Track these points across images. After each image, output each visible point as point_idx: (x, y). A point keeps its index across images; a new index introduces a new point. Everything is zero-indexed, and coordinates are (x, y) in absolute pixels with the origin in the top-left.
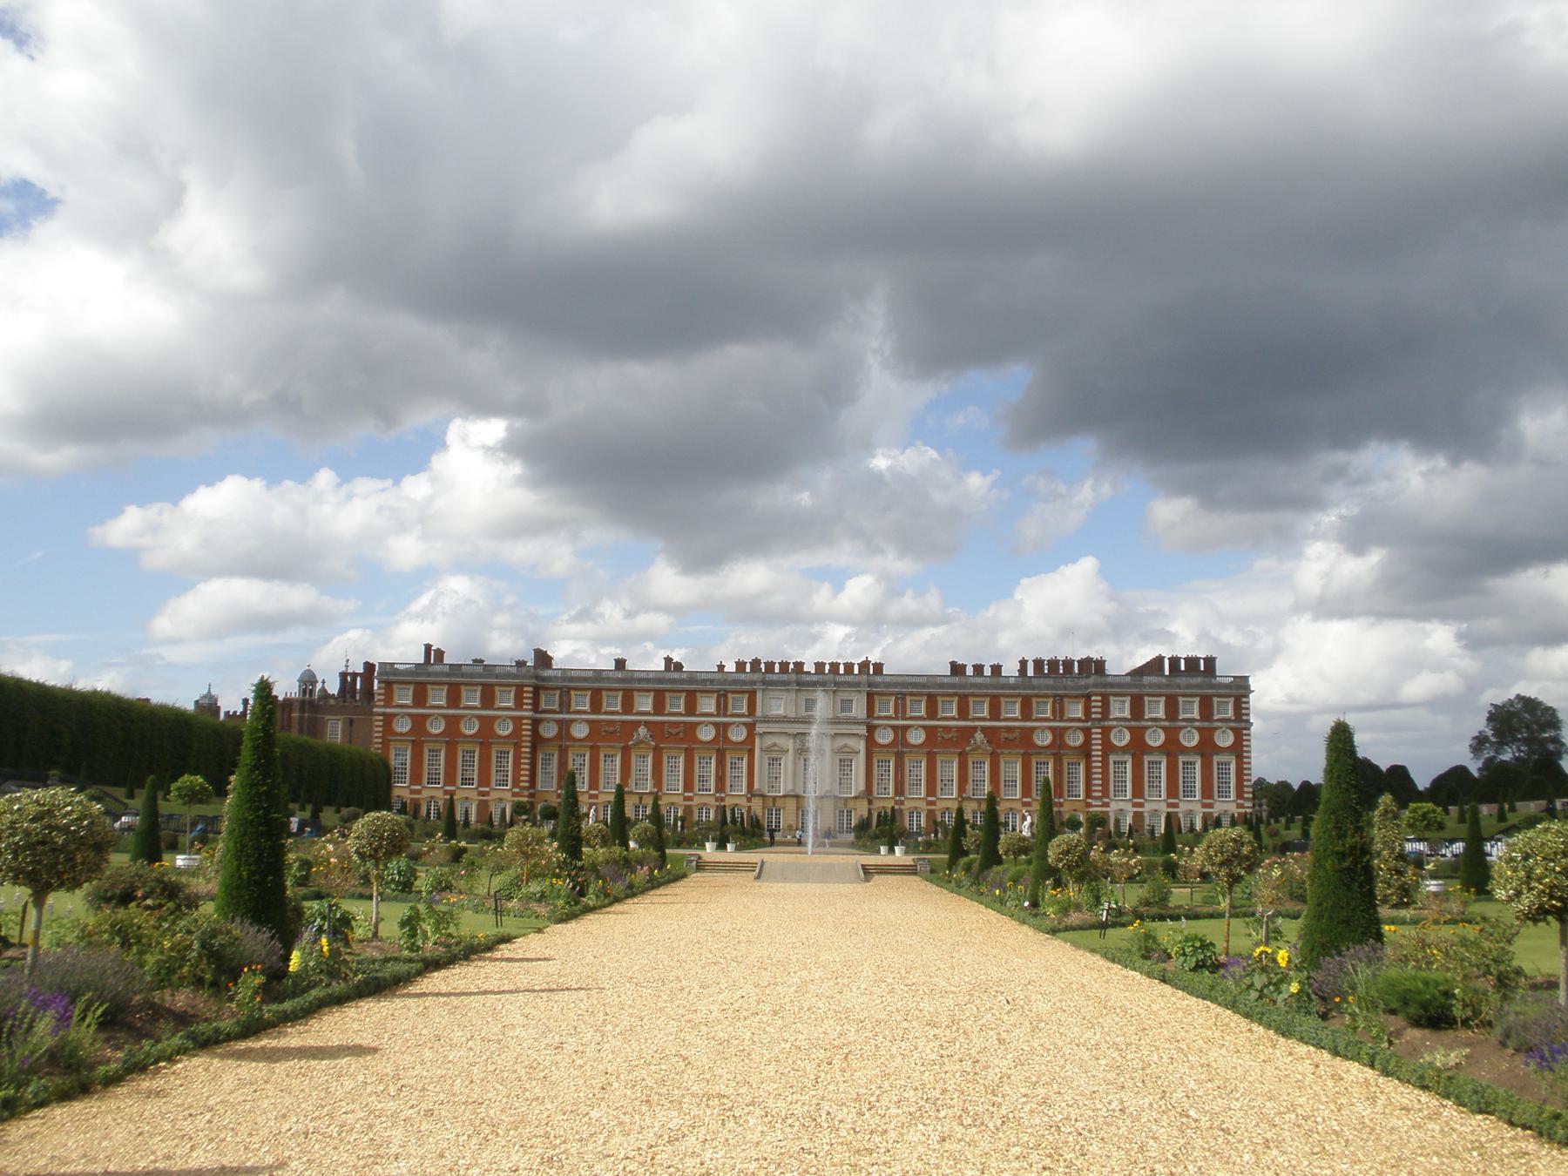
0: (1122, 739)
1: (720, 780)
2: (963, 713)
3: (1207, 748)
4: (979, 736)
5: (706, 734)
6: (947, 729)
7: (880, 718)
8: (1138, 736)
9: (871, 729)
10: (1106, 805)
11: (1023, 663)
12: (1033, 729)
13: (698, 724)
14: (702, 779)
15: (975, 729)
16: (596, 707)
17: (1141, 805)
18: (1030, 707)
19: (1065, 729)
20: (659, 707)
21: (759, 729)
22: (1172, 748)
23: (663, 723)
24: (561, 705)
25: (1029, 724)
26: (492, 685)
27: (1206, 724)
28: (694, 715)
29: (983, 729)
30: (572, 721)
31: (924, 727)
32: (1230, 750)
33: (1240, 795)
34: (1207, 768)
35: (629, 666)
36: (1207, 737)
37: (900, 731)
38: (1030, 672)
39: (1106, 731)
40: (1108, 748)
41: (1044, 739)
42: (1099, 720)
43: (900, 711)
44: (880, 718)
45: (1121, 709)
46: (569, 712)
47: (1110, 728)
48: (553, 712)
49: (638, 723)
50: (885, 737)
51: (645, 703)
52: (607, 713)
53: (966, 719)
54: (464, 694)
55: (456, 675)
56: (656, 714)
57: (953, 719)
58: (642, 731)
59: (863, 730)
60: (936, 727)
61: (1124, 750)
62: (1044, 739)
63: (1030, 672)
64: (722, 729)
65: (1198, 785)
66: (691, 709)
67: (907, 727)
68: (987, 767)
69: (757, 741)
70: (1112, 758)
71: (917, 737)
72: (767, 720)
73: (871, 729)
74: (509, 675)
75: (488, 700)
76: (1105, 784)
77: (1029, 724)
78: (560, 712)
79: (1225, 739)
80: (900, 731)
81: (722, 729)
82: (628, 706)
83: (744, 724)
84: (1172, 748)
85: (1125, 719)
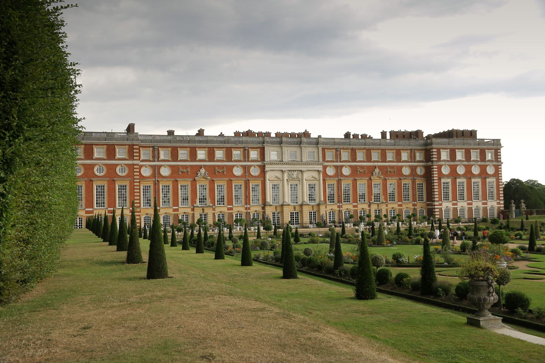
0: (445, 171)
1: (247, 197)
2: (369, 158)
3: (484, 175)
4: (377, 170)
5: (238, 172)
6: (362, 167)
7: (328, 161)
8: (453, 169)
9: (325, 167)
10: (441, 205)
11: (384, 134)
12: (402, 167)
13: (234, 166)
14: (237, 198)
15: (375, 167)
16: (175, 156)
17: (456, 204)
18: (400, 155)
19: (416, 167)
20: (211, 156)
21: (267, 168)
22: (469, 175)
23: (214, 166)
24: (154, 157)
25: (400, 164)
26: (114, 145)
27: (483, 163)
28: (231, 161)
29: (379, 167)
30: (161, 166)
31: (350, 166)
32: (493, 176)
33: (498, 198)
34: (484, 183)
35: (206, 134)
36: (483, 169)
37: (338, 169)
38: (388, 137)
39: (440, 167)
40: (441, 176)
41: (406, 171)
42: (436, 161)
43: (338, 157)
44: (328, 161)
45: (444, 155)
46: (158, 161)
47: (441, 166)
48: (149, 161)
49: (201, 167)
50: (331, 172)
51: (201, 154)
52: (181, 161)
53: (371, 162)
54: (95, 150)
55: (88, 139)
56: (209, 161)
57: (364, 162)
58: (203, 171)
59: (320, 168)
60: (356, 166)
61: (447, 176)
62: (406, 171)
63: (388, 137)
64: (246, 169)
65: (480, 193)
66: (229, 156)
67: (342, 167)
68: (381, 186)
69: (268, 176)
70: (443, 180)
71: (346, 171)
72: (272, 163)
73: (325, 167)
74: (122, 138)
75: (111, 153)
76: (440, 194)
77: (400, 164)
78: (154, 161)
79: (490, 170)
80: (338, 169)
81: (246, 169)
82: (193, 155)
83: (259, 166)
84: (469, 175)
85: (448, 161)
